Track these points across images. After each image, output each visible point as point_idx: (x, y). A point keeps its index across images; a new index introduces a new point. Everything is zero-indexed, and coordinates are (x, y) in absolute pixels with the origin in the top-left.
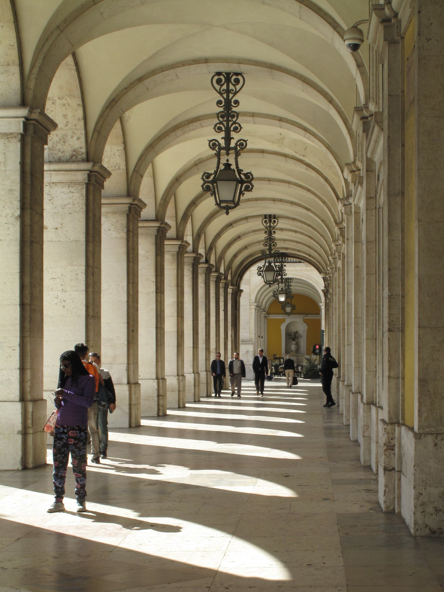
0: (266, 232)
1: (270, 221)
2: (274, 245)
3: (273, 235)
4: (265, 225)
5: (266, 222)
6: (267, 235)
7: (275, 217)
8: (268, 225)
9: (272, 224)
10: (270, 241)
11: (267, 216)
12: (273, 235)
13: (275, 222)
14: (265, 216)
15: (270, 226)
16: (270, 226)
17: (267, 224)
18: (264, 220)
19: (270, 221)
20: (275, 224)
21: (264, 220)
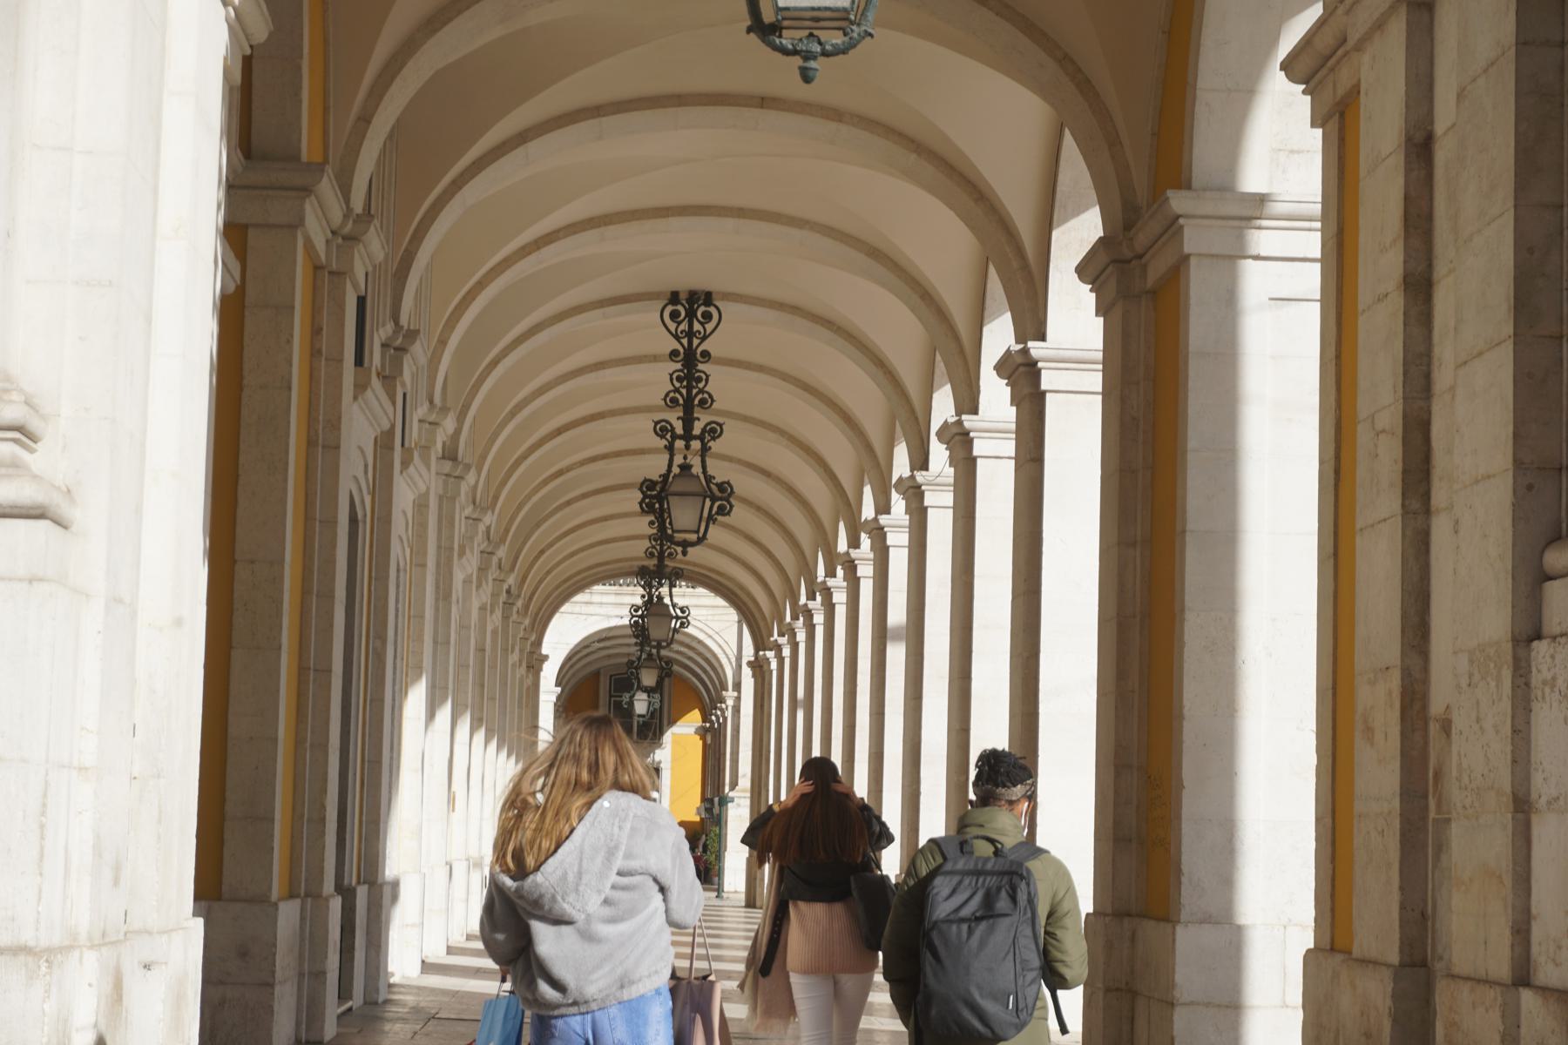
0: (674, 353)
1: (691, 315)
2: (703, 402)
3: (700, 367)
4: (672, 326)
5: (674, 315)
6: (679, 366)
7: (708, 298)
8: (684, 326)
9: (697, 326)
10: (689, 388)
11: (683, 297)
12: (700, 367)
13: (708, 317)
14: (674, 298)
15: (690, 334)
16: (690, 334)
17: (679, 323)
18: (670, 308)
19: (691, 315)
20: (709, 327)
21: (670, 308)
